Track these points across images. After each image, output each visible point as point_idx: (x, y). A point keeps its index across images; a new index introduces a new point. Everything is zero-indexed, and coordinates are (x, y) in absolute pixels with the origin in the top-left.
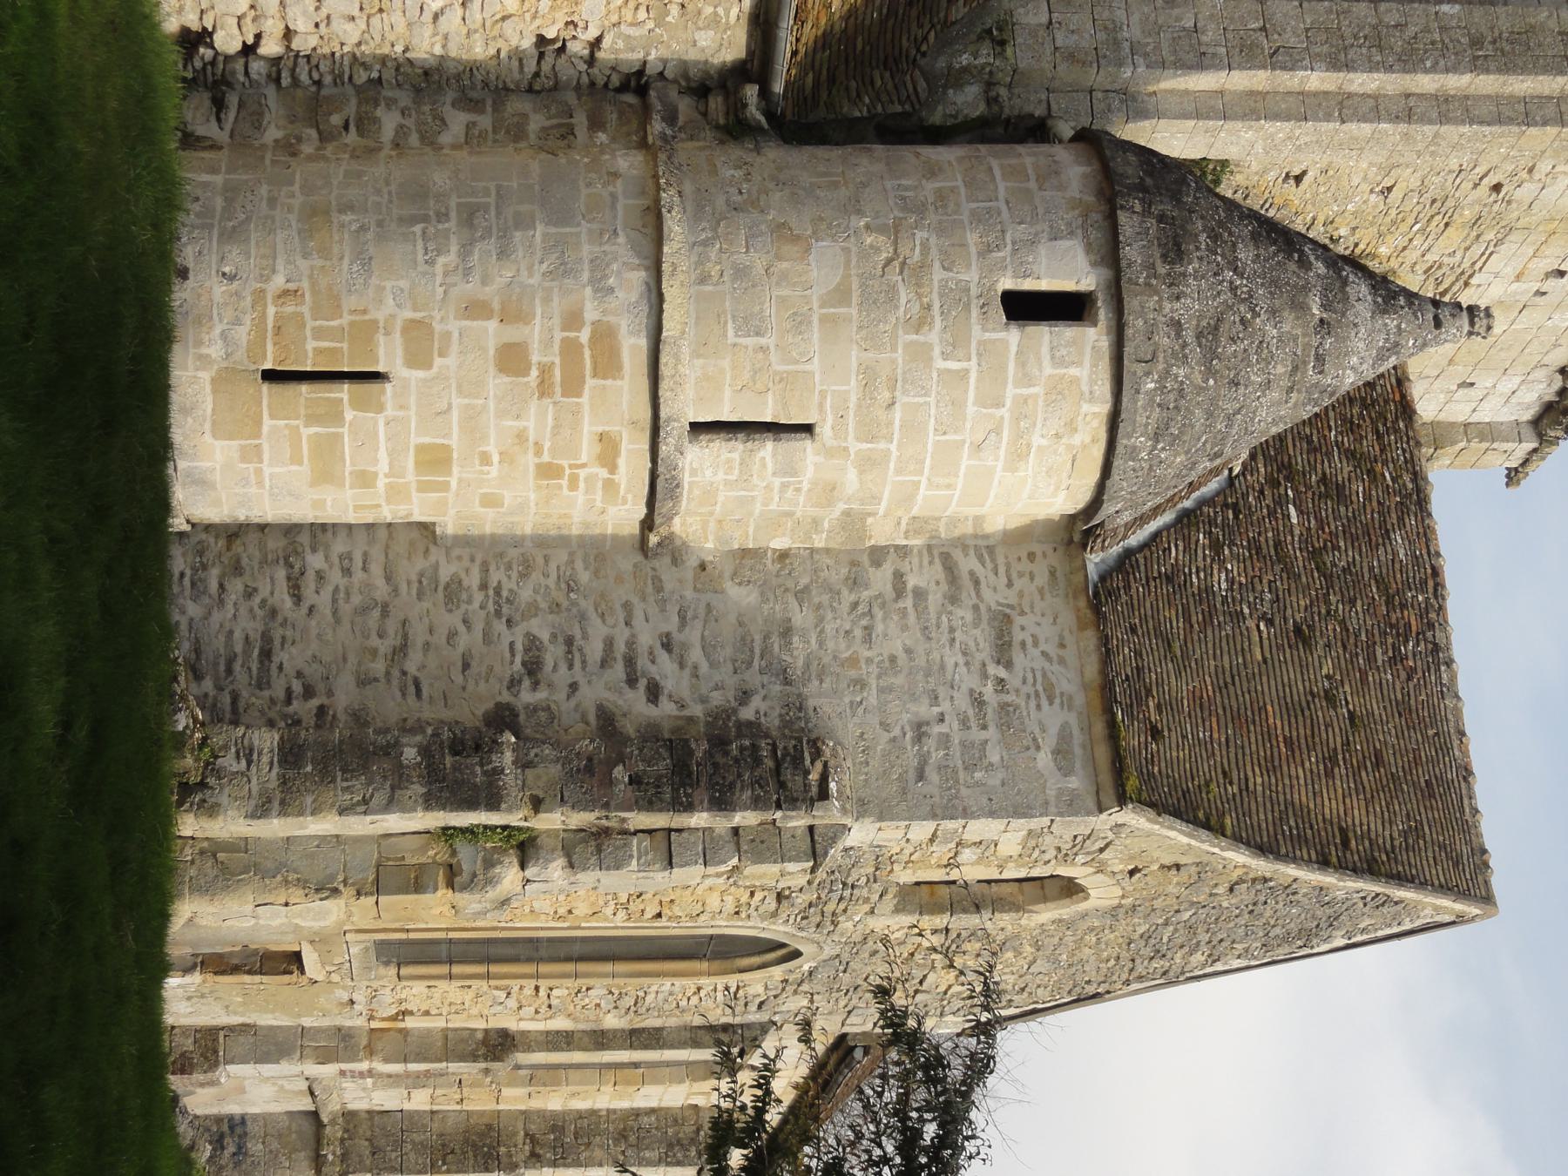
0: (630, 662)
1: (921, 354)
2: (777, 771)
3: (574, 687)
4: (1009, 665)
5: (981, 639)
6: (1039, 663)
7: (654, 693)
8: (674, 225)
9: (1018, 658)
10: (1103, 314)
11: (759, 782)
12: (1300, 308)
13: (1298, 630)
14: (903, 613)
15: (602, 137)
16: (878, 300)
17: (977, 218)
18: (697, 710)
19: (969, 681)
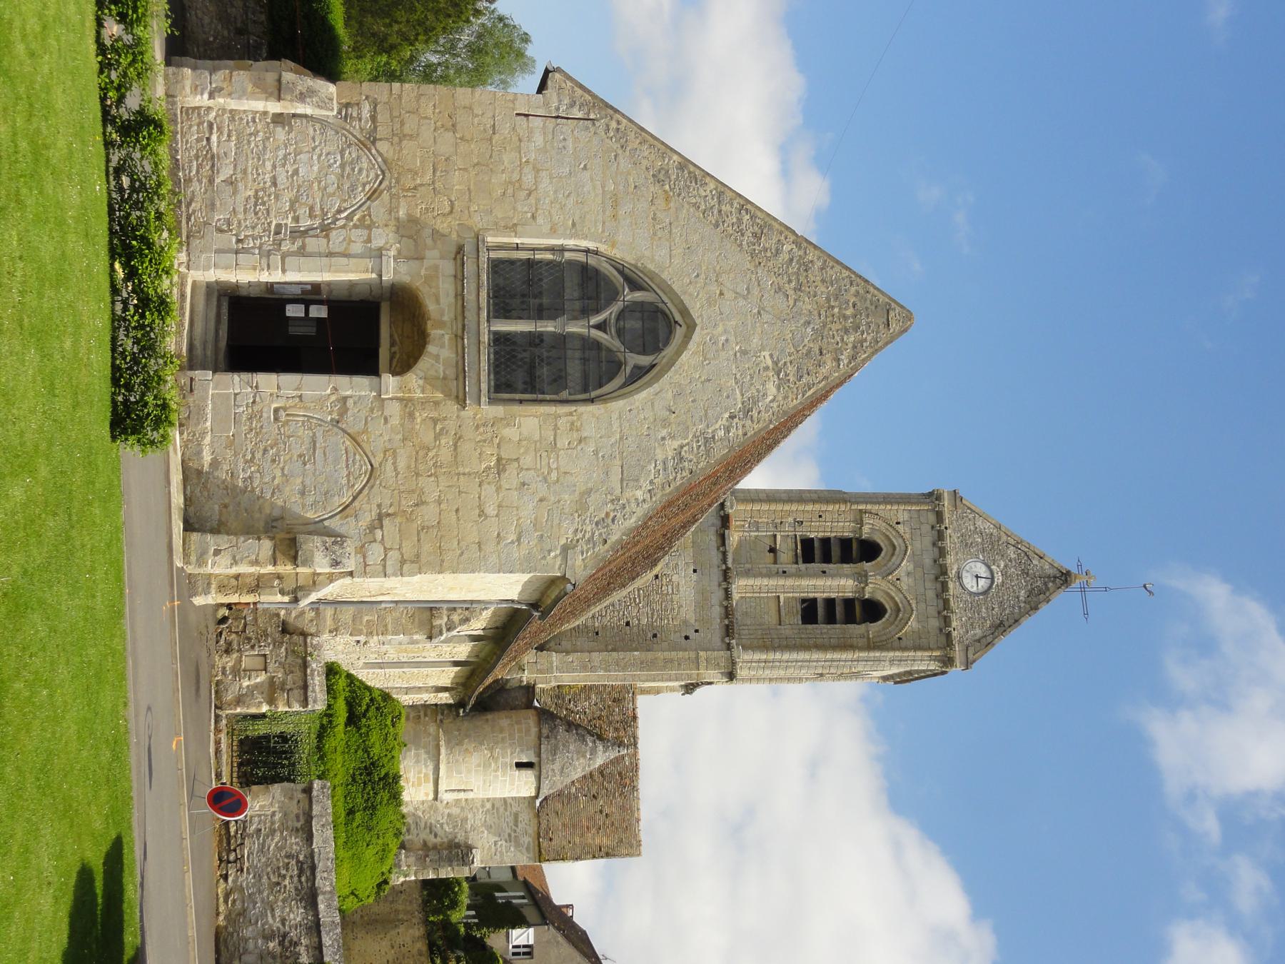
0: (430, 828)
1: (496, 777)
2: (463, 858)
3: (418, 835)
4: (517, 826)
5: (511, 820)
6: (525, 826)
7: (436, 836)
8: (443, 750)
9: (519, 824)
10: (537, 767)
11: (458, 860)
12: (584, 756)
13: (594, 796)
14: (493, 814)
15: (427, 719)
16: (486, 766)
17: (510, 745)
18: (446, 840)
19: (508, 831)
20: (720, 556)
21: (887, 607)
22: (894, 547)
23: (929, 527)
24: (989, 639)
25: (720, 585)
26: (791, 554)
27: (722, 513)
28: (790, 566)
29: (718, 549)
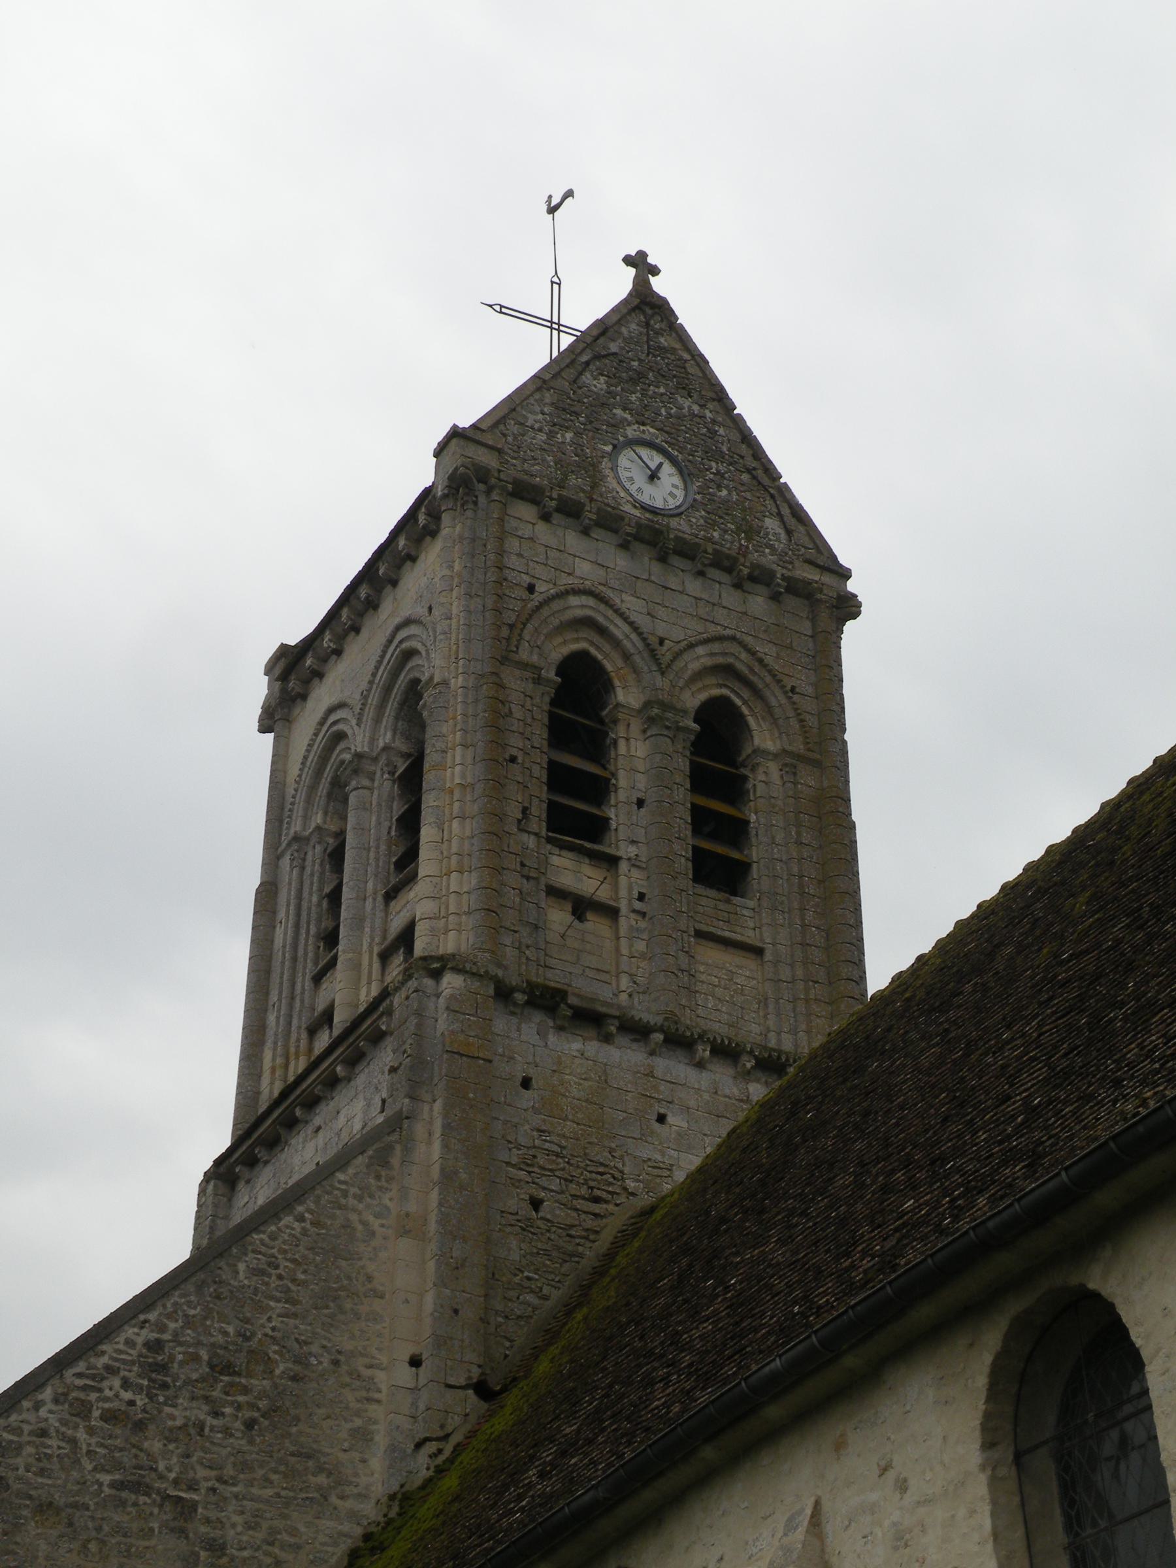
20: (623, 1040)
21: (716, 692)
22: (588, 623)
23: (541, 527)
24: (786, 511)
25: (700, 1065)
26: (587, 869)
27: (520, 997)
28: (623, 880)
29: (607, 1039)
